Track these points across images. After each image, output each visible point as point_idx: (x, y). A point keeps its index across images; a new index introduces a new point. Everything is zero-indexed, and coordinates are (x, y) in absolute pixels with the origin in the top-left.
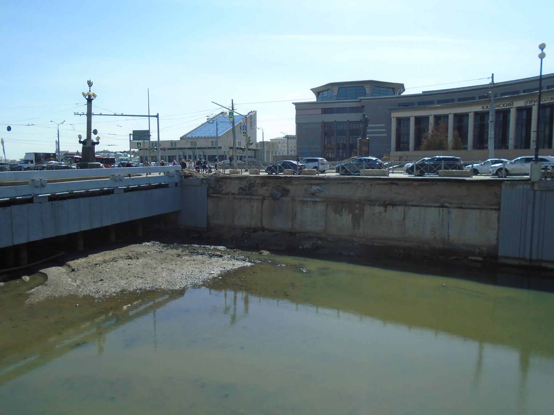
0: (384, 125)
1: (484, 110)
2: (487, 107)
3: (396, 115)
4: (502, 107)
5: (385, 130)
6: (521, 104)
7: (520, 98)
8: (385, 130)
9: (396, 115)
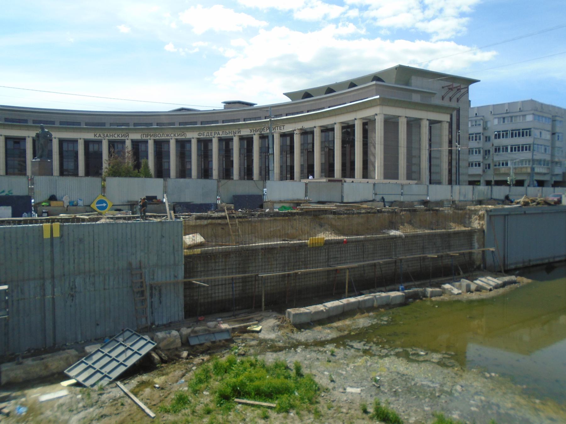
1: (96, 138)
2: (100, 136)
4: (116, 137)
6: (137, 136)
7: (135, 130)
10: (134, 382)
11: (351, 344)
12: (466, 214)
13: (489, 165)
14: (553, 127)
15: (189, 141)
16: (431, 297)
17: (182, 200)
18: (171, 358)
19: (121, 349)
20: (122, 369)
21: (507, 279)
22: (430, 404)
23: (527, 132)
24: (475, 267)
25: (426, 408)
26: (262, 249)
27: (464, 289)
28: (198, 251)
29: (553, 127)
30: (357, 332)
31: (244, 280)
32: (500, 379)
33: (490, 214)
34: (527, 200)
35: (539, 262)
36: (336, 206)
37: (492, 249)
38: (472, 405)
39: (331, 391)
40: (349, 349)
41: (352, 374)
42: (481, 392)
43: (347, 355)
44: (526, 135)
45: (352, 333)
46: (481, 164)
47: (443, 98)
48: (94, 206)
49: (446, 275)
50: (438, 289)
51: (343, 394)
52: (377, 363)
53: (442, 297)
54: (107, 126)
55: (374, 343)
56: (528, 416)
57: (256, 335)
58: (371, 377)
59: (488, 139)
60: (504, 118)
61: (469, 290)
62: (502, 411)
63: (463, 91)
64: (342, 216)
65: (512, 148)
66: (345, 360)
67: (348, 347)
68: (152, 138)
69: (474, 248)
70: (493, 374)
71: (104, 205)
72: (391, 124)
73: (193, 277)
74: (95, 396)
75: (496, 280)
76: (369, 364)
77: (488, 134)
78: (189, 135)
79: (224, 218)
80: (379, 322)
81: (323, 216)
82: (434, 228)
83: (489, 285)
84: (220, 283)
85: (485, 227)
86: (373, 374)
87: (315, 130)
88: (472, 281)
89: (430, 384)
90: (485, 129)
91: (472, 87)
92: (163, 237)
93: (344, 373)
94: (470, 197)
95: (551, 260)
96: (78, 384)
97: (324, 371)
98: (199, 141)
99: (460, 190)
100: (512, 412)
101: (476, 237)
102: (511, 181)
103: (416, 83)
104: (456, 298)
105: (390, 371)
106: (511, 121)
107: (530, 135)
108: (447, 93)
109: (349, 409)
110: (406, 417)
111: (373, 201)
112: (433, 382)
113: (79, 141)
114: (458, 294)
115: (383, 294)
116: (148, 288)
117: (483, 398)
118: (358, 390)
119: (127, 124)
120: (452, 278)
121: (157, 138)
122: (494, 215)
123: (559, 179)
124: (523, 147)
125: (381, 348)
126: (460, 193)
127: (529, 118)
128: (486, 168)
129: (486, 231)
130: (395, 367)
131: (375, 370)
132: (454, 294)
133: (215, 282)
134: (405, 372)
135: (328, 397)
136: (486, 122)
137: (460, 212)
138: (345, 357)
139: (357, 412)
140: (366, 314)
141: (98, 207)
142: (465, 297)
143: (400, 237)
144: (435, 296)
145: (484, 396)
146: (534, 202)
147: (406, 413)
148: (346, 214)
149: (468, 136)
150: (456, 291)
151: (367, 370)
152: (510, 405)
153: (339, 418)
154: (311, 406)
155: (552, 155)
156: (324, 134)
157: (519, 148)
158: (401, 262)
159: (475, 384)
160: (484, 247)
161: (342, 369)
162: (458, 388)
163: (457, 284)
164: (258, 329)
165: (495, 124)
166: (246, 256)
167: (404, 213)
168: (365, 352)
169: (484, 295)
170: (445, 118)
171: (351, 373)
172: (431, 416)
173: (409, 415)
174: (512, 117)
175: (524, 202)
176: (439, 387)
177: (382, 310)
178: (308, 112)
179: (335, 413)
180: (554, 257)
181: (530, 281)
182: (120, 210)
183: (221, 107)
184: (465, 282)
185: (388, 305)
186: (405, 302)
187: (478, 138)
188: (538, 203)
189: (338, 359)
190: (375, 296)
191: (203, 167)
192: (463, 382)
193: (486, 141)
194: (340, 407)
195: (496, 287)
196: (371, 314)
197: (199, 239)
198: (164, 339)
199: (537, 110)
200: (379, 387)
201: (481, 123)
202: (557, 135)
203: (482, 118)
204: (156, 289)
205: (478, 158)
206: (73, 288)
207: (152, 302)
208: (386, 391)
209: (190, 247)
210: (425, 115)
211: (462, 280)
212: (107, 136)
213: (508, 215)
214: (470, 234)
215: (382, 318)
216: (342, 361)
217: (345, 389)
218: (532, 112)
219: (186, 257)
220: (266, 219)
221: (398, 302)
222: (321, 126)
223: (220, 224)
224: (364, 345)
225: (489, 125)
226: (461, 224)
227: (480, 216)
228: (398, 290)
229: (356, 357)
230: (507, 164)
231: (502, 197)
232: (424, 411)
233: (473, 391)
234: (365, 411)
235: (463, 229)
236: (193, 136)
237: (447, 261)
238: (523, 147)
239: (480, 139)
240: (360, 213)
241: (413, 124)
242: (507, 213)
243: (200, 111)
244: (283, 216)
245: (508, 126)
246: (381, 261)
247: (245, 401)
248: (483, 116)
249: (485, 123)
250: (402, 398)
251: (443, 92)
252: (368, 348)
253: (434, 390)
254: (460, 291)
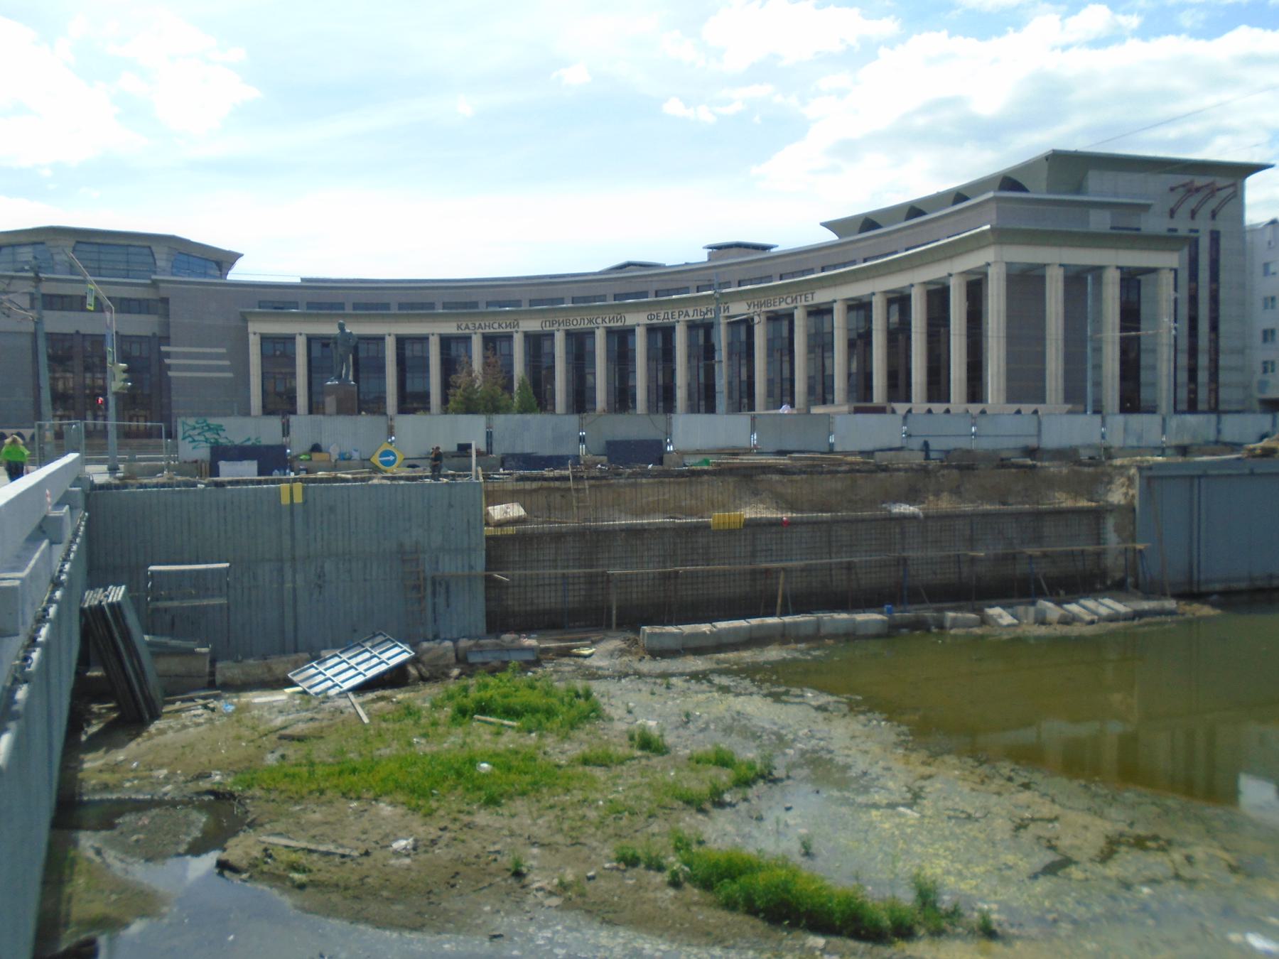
0: (223, 350)
2: (467, 327)
3: (257, 328)
4: (496, 328)
5: (227, 363)
6: (533, 325)
7: (530, 314)
8: (227, 363)
9: (257, 328)
10: (370, 696)
15: (631, 331)
17: (518, 450)
18: (435, 675)
19: (367, 655)
20: (360, 679)
24: (1109, 582)
26: (622, 530)
28: (510, 530)
31: (591, 580)
36: (791, 458)
47: (1172, 213)
48: (376, 460)
54: (482, 308)
57: (581, 660)
61: (1042, 621)
64: (795, 477)
68: (562, 327)
71: (392, 458)
72: (1026, 283)
73: (496, 570)
74: (315, 703)
78: (631, 319)
79: (566, 479)
81: (762, 477)
84: (547, 582)
85: (1137, 503)
87: (874, 299)
92: (450, 506)
96: (304, 692)
98: (651, 329)
99: (1126, 424)
103: (1099, 187)
108: (1180, 203)
111: (900, 449)
113: (431, 338)
116: (429, 582)
119: (517, 303)
121: (572, 327)
122: (1162, 478)
126: (1125, 430)
132: (1000, 626)
133: (546, 580)
141: (382, 462)
143: (913, 517)
144: (958, 627)
148: (805, 473)
156: (812, 319)
164: (586, 652)
166: (596, 539)
169: (1075, 630)
178: (865, 260)
182: (413, 466)
183: (701, 256)
186: (890, 632)
191: (661, 382)
197: (516, 510)
198: (429, 650)
204: (442, 585)
206: (321, 575)
207: (434, 604)
209: (500, 524)
210: (1113, 259)
212: (480, 326)
213: (1199, 477)
214: (1097, 515)
219: (488, 538)
220: (644, 481)
222: (886, 292)
223: (558, 489)
236: (637, 320)
240: (838, 472)
241: (1077, 280)
243: (663, 266)
244: (677, 476)
247: (489, 719)
251: (1173, 200)
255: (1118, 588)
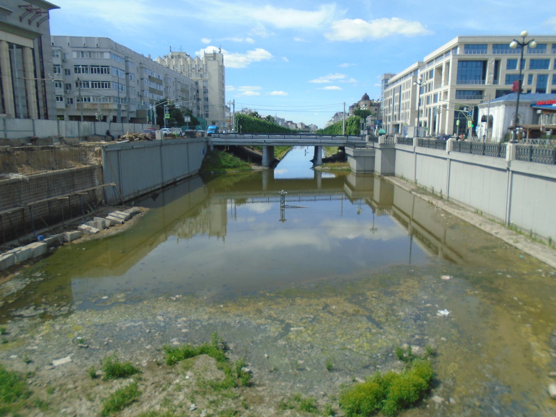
11: (18, 313)
12: (82, 150)
13: (71, 99)
14: (127, 67)
16: (72, 241)
21: (131, 210)
22: (147, 342)
23: (105, 69)
25: (148, 347)
27: (100, 225)
29: (127, 67)
30: (15, 298)
32: (185, 298)
33: (107, 150)
34: (131, 136)
35: (145, 192)
37: (112, 184)
38: (180, 329)
39: (37, 373)
40: (19, 320)
41: (46, 346)
42: (179, 314)
43: (23, 327)
44: (105, 73)
45: (10, 301)
46: (63, 99)
47: (21, 19)
49: (75, 216)
50: (76, 232)
51: (53, 370)
52: (65, 323)
53: (83, 239)
55: (45, 304)
56: (223, 320)
58: (71, 340)
59: (67, 72)
60: (82, 52)
62: (205, 323)
63: (44, 15)
65: (92, 84)
66: (26, 334)
67: (16, 318)
69: (95, 185)
70: (177, 296)
75: (123, 213)
76: (57, 328)
77: (67, 67)
80: (33, 280)
82: (55, 167)
83: (121, 219)
86: (71, 337)
88: (105, 218)
89: (133, 324)
90: (64, 61)
91: (52, 12)
93: (36, 347)
94: (76, 133)
95: (153, 189)
97: (8, 355)
100: (211, 321)
101: (96, 174)
102: (99, 116)
104: (97, 237)
105: (86, 326)
106: (90, 57)
107: (108, 73)
109: (75, 382)
110: (137, 363)
112: (135, 322)
114: (98, 232)
115: (24, 248)
117: (184, 319)
118: (68, 359)
120: (82, 217)
122: (110, 151)
123: (134, 116)
124: (103, 84)
125: (57, 306)
127: (107, 56)
128: (69, 103)
129: (104, 167)
130: (89, 321)
131: (70, 332)
132: (94, 233)
134: (103, 321)
135: (38, 381)
136: (65, 54)
137: (77, 148)
138: (22, 330)
139: (85, 381)
140: (11, 276)
142: (105, 234)
143: (23, 181)
144: (76, 239)
145: (184, 317)
146: (136, 137)
147: (134, 359)
149: (52, 67)
150: (94, 230)
151: (60, 334)
152: (206, 317)
153: (71, 397)
154: (28, 400)
155: (128, 93)
157: (99, 84)
158: (30, 209)
159: (169, 309)
160: (103, 183)
161: (29, 344)
162: (160, 318)
163: (92, 222)
165: (73, 57)
167: (18, 152)
168: (44, 316)
169: (120, 229)
170: (28, 43)
171: (44, 344)
172: (157, 352)
173: (137, 359)
174: (90, 52)
175: (129, 137)
176: (143, 323)
177: (27, 266)
179: (62, 394)
180: (154, 187)
181: (148, 209)
184: (99, 220)
185: (31, 259)
187: (57, 70)
188: (140, 139)
189: (16, 336)
190: (14, 253)
192: (160, 312)
193: (66, 74)
194: (61, 385)
195: (127, 219)
196: (17, 274)
199: (112, 49)
200: (88, 347)
201: (59, 54)
202: (130, 75)
203: (59, 48)
205: (60, 91)
208: (98, 347)
211: (95, 218)
213: (120, 150)
214: (91, 171)
215: (33, 275)
216: (22, 336)
217: (51, 364)
218: (109, 50)
221: (41, 253)
224: (35, 309)
225: (68, 57)
226: (80, 161)
227: (96, 152)
228: (36, 240)
229: (36, 326)
230: (89, 100)
231: (104, 133)
232: (148, 350)
233: (173, 316)
234: (94, 376)
235: (85, 166)
237: (74, 202)
238: (103, 84)
239: (59, 72)
242: (119, 149)
245: (88, 62)
246: (9, 211)
248: (61, 47)
249: (64, 55)
250: (118, 347)
251: (21, 12)
252: (42, 311)
253: (141, 328)
254: (98, 230)
255: (122, 204)
